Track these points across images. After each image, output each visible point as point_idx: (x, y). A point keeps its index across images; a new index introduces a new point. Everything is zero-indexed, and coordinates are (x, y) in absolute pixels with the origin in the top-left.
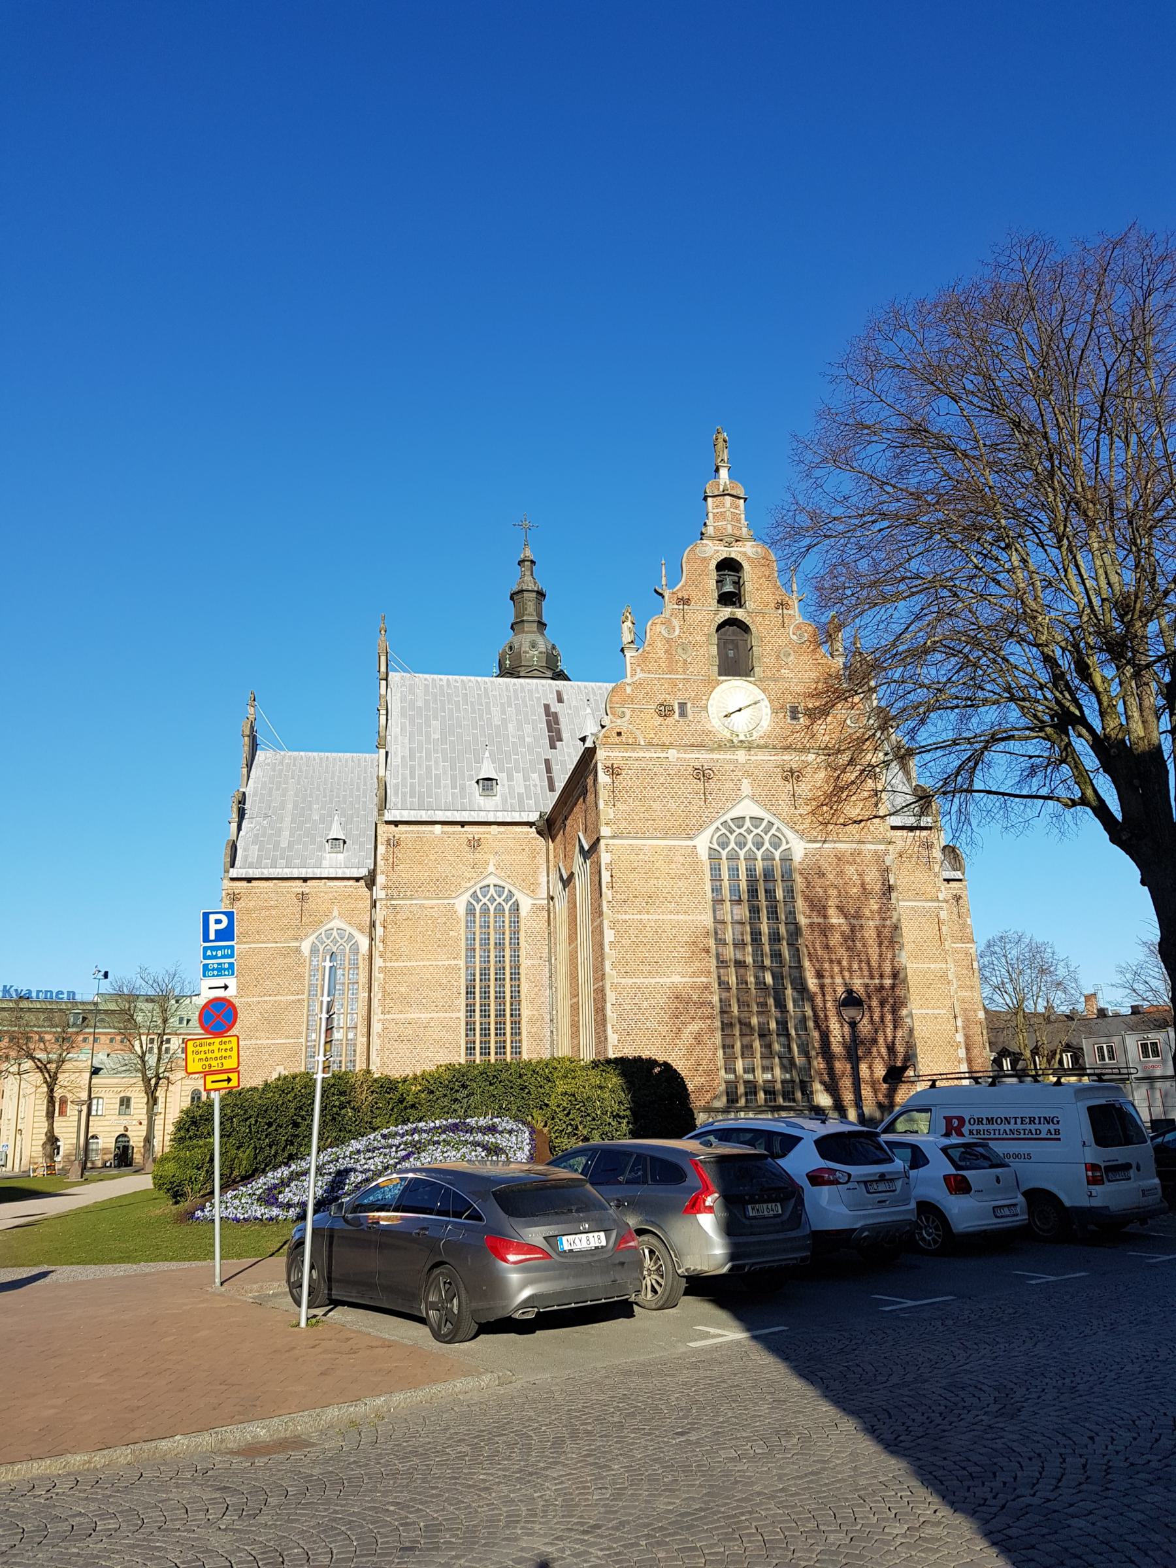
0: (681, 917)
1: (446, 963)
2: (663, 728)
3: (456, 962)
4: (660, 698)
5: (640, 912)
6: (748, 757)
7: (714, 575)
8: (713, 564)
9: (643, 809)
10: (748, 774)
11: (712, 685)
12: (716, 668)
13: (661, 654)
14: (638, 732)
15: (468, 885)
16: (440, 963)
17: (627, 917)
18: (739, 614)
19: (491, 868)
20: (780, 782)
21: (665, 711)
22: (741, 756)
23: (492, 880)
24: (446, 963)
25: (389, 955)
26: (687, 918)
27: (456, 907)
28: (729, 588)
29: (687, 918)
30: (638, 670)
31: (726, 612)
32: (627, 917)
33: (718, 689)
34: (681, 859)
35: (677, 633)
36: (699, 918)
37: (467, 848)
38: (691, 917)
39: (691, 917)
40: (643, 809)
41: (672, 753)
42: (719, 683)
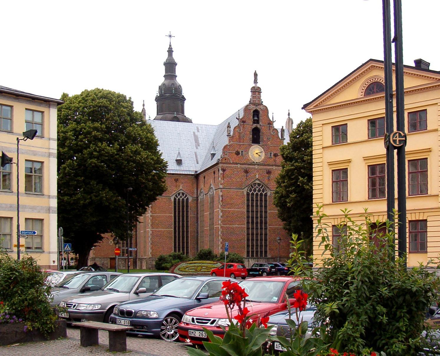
5: (229, 208)
8: (252, 111)
9: (231, 181)
12: (251, 141)
13: (237, 137)
15: (175, 192)
17: (226, 209)
18: (258, 126)
19: (181, 188)
21: (238, 153)
23: (181, 191)
25: (154, 212)
27: (171, 199)
28: (256, 118)
29: (240, 210)
31: (255, 125)
32: (226, 209)
35: (242, 131)
37: (174, 182)
41: (239, 166)
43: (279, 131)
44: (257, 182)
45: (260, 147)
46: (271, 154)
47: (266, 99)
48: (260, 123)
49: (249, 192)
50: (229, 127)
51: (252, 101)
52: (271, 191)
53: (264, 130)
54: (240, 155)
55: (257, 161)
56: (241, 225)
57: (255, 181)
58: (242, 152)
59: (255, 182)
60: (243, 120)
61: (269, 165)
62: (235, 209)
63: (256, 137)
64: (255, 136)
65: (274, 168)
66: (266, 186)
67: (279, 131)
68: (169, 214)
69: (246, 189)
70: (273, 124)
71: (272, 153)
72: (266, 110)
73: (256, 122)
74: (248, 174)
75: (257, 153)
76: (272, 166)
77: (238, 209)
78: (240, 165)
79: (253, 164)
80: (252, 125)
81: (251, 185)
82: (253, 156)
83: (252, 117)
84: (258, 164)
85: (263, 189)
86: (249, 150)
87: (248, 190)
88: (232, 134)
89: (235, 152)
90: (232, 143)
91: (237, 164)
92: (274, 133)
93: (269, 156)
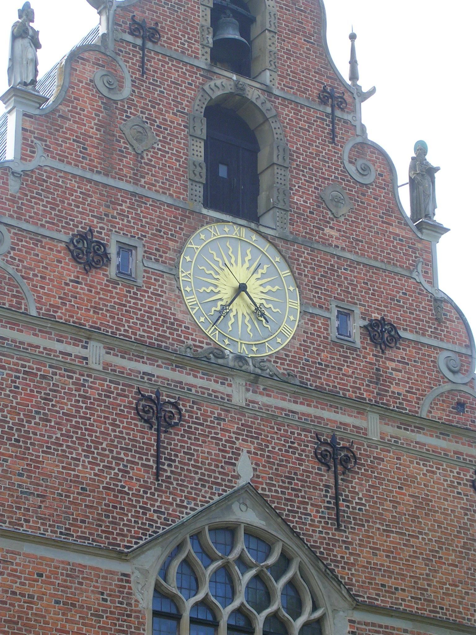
2: (82, 289)
4: (82, 221)
6: (250, 395)
9: (21, 465)
10: (249, 432)
11: (192, 222)
12: (199, 190)
14: (25, 286)
18: (253, 93)
20: (310, 465)
21: (88, 253)
22: (238, 393)
28: (232, 34)
31: (225, 81)
34: (94, 599)
35: (127, 91)
40: (21, 465)
41: (96, 353)
42: (204, 221)
43: (403, 175)
44: (247, 515)
45: (266, 247)
46: (345, 315)
48: (267, 77)
49: (172, 587)
50: (25, 33)
52: (358, 616)
53: (288, 131)
54: (112, 271)
55: (242, 350)
57: (226, 502)
58: (126, 250)
59: (231, 518)
61: (331, 397)
63: (235, 170)
64: (223, 171)
65: (374, 426)
66: (317, 559)
67: (403, 175)
69: (151, 560)
70: (355, 110)
71: (358, 311)
73: (235, 55)
74: (174, 439)
75: (242, 288)
76: (359, 406)
78: (109, 349)
79: (211, 360)
80: (209, 74)
81: (197, 537)
83: (204, 17)
84: (258, 375)
85: (291, 584)
87: (164, 572)
89: (66, 238)
90: (40, 159)
91: (83, 334)
93: (334, 334)
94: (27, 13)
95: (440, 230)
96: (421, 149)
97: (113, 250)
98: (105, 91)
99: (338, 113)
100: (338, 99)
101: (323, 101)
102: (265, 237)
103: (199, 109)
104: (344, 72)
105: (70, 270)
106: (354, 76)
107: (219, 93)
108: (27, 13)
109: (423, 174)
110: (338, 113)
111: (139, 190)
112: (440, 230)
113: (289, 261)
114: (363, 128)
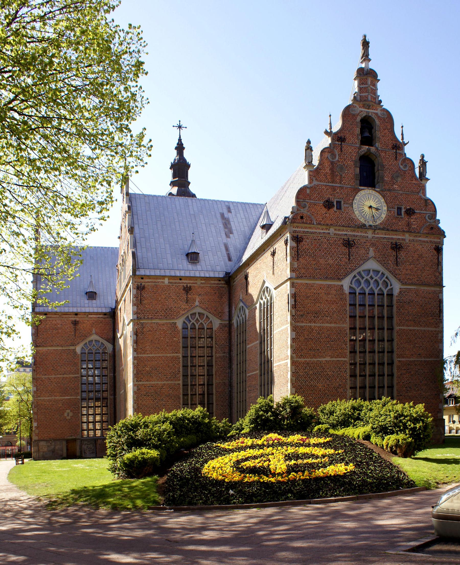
0: (333, 325)
1: (172, 355)
3: (177, 355)
6: (373, 235)
7: (359, 125)
8: (359, 119)
12: (358, 182)
13: (328, 170)
16: (168, 355)
21: (328, 205)
24: (172, 355)
26: (336, 325)
28: (367, 134)
29: (336, 325)
30: (314, 180)
33: (359, 194)
34: (334, 292)
35: (337, 158)
36: (342, 325)
38: (338, 325)
39: (338, 325)
45: (377, 194)
47: (389, 96)
50: (309, 149)
51: (358, 98)
56: (338, 356)
60: (339, 135)
62: (323, 323)
68: (173, 353)
70: (403, 149)
72: (388, 118)
73: (367, 140)
75: (370, 207)
77: (331, 323)
82: (361, 212)
83: (358, 131)
86: (353, 200)
88: (316, 162)
90: (315, 183)
92: (406, 166)
94: (309, 142)
95: (428, 179)
96: (423, 156)
97: (335, 203)
98: (331, 160)
99: (398, 151)
100: (398, 147)
101: (393, 148)
102: (377, 191)
103: (357, 158)
104: (399, 138)
105: (324, 210)
106: (403, 139)
107: (363, 153)
108: (309, 142)
109: (423, 163)
110: (398, 151)
111: (341, 185)
112: (428, 179)
113: (384, 197)
114: (405, 154)
